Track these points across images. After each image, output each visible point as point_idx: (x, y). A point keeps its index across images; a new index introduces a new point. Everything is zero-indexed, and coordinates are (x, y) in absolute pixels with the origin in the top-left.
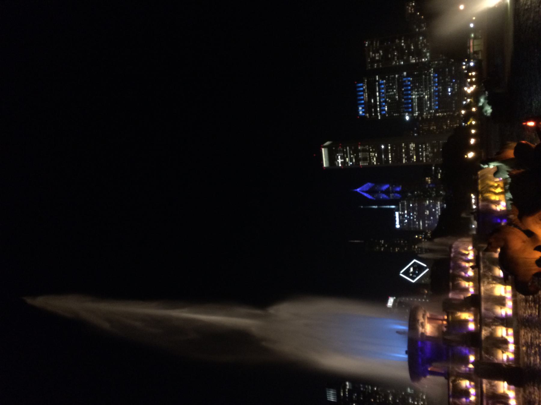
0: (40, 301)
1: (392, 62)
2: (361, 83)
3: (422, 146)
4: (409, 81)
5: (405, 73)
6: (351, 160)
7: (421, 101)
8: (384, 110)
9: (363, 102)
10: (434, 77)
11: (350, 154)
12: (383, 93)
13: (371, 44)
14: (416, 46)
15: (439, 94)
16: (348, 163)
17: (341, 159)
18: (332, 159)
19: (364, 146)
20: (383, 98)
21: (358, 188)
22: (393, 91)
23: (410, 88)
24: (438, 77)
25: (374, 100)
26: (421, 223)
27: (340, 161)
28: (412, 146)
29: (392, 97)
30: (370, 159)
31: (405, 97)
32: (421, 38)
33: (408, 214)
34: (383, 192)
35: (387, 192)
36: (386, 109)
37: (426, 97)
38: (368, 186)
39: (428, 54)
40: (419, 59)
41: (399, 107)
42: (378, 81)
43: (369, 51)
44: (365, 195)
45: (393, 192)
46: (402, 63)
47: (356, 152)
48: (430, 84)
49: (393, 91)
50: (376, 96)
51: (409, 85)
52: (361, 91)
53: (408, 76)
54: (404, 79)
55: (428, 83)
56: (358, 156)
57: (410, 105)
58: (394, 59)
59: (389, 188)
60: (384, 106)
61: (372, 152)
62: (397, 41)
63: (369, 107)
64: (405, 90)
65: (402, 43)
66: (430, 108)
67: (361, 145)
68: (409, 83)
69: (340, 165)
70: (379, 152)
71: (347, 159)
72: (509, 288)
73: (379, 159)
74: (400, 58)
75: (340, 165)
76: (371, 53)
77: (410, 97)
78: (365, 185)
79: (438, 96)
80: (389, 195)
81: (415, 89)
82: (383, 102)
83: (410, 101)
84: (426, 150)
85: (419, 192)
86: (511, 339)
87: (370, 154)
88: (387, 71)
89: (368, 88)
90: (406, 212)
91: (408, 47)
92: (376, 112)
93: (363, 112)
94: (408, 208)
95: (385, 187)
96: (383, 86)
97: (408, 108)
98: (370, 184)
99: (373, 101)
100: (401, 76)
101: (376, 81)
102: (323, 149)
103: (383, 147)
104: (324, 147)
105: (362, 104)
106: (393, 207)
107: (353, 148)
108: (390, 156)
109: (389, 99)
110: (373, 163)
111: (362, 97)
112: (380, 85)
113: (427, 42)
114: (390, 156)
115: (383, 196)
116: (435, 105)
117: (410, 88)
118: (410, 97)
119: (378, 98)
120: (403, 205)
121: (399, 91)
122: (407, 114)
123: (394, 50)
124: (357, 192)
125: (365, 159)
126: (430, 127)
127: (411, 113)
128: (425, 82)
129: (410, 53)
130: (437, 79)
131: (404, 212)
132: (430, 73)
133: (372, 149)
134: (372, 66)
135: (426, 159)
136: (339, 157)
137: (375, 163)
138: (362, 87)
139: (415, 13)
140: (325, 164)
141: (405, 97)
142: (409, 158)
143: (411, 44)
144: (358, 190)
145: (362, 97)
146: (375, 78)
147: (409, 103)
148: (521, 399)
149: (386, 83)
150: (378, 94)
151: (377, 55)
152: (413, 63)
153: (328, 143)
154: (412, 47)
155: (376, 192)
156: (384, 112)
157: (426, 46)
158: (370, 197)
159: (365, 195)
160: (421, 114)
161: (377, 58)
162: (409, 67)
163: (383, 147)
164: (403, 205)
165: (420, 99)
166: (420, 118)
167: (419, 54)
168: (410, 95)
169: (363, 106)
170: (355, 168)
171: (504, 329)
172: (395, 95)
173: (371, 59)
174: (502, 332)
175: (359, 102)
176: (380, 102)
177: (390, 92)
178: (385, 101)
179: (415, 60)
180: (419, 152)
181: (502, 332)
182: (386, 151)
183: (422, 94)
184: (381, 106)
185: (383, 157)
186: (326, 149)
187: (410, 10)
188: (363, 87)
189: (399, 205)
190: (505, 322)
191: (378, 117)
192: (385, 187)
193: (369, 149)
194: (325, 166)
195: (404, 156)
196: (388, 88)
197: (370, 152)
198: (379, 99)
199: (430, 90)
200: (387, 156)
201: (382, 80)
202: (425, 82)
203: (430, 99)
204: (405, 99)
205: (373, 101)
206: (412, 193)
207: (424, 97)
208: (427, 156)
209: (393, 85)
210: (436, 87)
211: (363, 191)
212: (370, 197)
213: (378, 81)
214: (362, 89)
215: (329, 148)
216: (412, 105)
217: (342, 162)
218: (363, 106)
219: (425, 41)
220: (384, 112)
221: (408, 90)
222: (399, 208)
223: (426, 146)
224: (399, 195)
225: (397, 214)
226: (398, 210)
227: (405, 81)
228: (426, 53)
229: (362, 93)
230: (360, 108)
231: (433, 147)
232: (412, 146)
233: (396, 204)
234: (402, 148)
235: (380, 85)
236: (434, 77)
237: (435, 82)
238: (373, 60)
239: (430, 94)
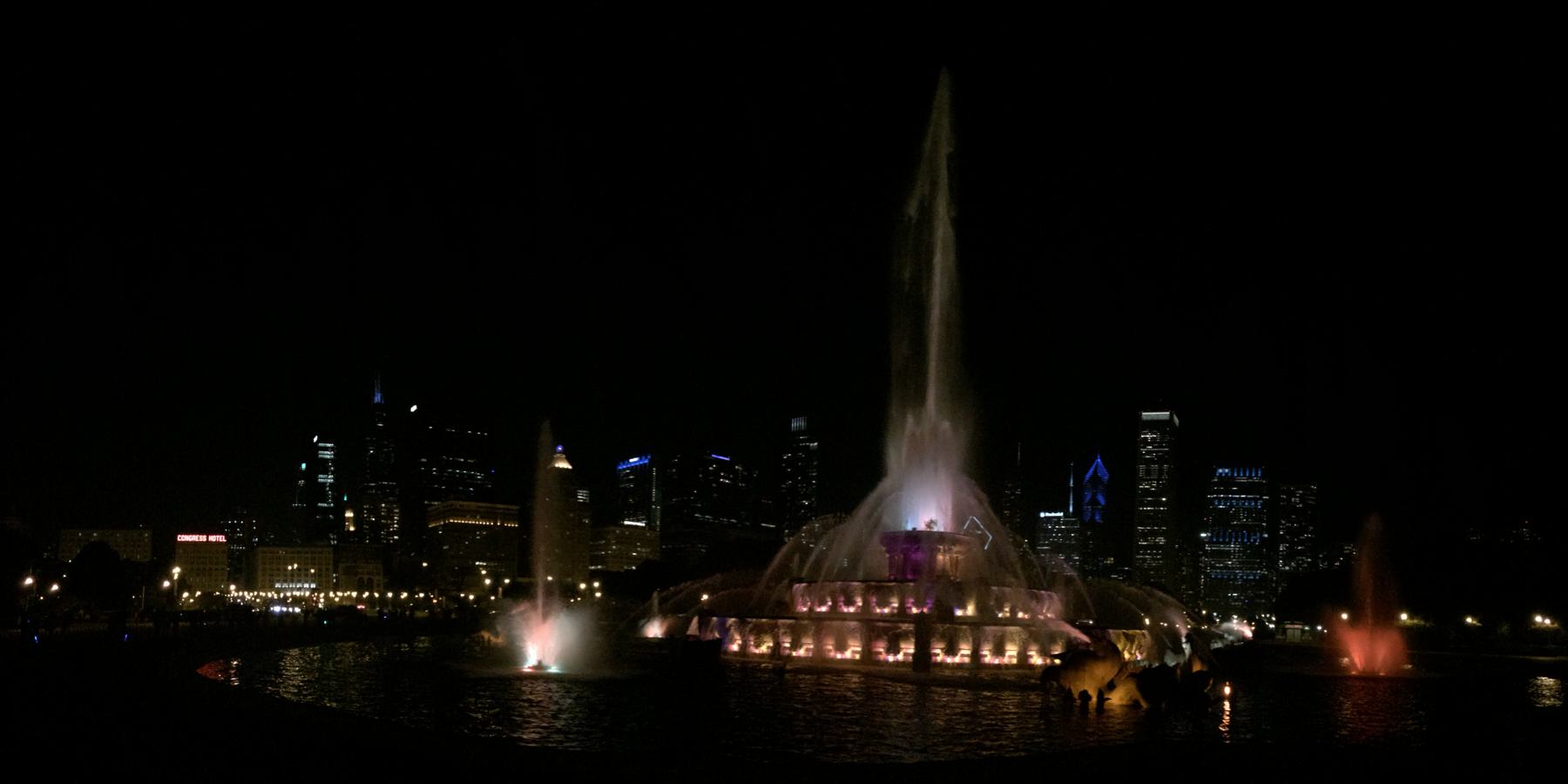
6: (1149, 452)
7: (1227, 556)
14: (1301, 553)
18: (1153, 425)
25: (1235, 489)
28: (1161, 541)
29: (1236, 516)
33: (1060, 530)
35: (1094, 502)
38: (1105, 475)
41: (1222, 524)
47: (1160, 460)
53: (1262, 539)
63: (1227, 483)
66: (1213, 567)
72: (1015, 661)
73: (1147, 492)
74: (1288, 531)
86: (957, 659)
92: (1219, 492)
94: (1069, 531)
95: (1101, 499)
100: (1263, 530)
112: (1256, 500)
120: (1073, 523)
121: (1244, 526)
125: (1148, 472)
127: (1210, 542)
129: (1293, 544)
140: (1146, 415)
142: (1144, 536)
148: (840, 667)
153: (1176, 420)
158: (1088, 476)
160: (1206, 553)
162: (1275, 540)
164: (1073, 523)
165: (1227, 554)
167: (1288, 557)
171: (1015, 653)
174: (965, 650)
181: (965, 650)
184: (1226, 499)
190: (923, 653)
192: (1101, 499)
196: (1249, 511)
203: (1226, 567)
212: (1088, 476)
215: (1170, 421)
231: (1157, 569)
232: (1161, 541)
233: (1075, 514)
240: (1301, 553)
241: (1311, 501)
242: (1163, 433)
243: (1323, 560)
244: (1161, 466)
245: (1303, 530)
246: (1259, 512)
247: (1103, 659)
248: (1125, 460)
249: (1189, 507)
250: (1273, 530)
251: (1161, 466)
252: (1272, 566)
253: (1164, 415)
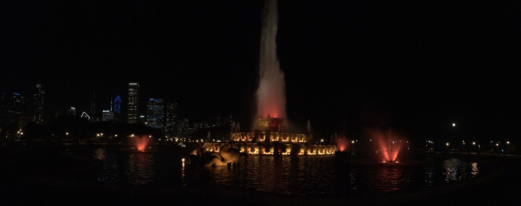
14: (173, 121)
35: (117, 108)
38: (120, 100)
47: (134, 96)
63: (152, 102)
70: (134, 106)
74: (169, 115)
95: (119, 107)
115: (116, 106)
125: (131, 100)
129: (170, 119)
142: (130, 117)
162: (166, 117)
165: (153, 121)
188: (160, 101)
192: (119, 107)
200: (132, 108)
238: (170, 106)
240: (173, 121)
248: (125, 96)
252: (165, 125)
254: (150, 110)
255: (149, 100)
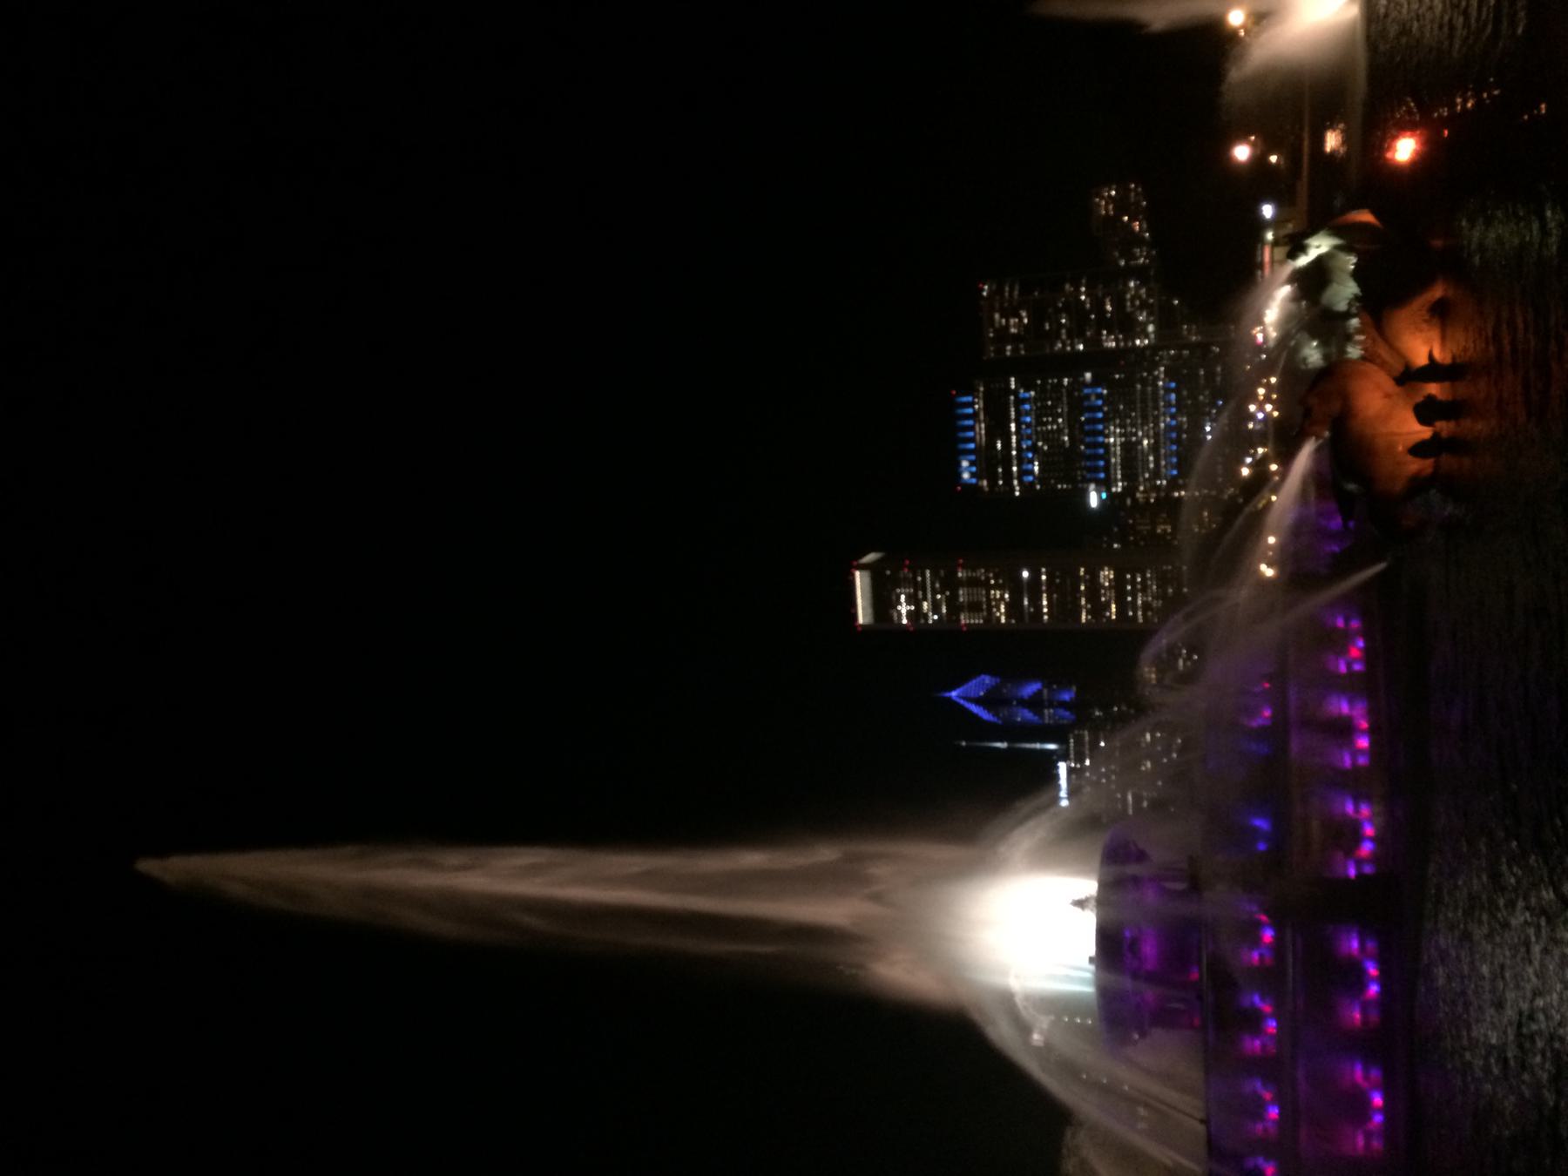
0: (173, 868)
1: (1053, 345)
2: (967, 394)
3: (1134, 578)
4: (1099, 396)
5: (1088, 376)
6: (936, 608)
8: (1031, 472)
9: (972, 446)
10: (1168, 390)
11: (934, 592)
12: (1028, 425)
13: (997, 292)
14: (1119, 303)
15: (1179, 436)
16: (926, 616)
17: (908, 602)
18: (882, 603)
19: (974, 570)
20: (1029, 437)
21: (954, 688)
22: (1055, 422)
23: (1100, 415)
24: (1177, 391)
25: (1002, 443)
26: (1130, 798)
27: (904, 609)
28: (1107, 575)
29: (1049, 437)
30: (991, 605)
31: (1088, 440)
32: (1132, 284)
34: (1024, 703)
35: (1035, 703)
36: (1036, 469)
37: (1146, 442)
38: (982, 683)
39: (1151, 328)
40: (1125, 340)
41: (1071, 465)
42: (1015, 393)
43: (992, 310)
44: (974, 709)
45: (1051, 705)
46: (1081, 347)
47: (950, 584)
48: (1156, 408)
49: (1055, 422)
50: (1009, 433)
51: (1099, 409)
52: (968, 417)
53: (1096, 382)
54: (1086, 391)
55: (1150, 404)
56: (954, 596)
57: (1102, 463)
58: (1058, 336)
59: (1040, 692)
60: (1031, 462)
61: (995, 587)
62: (1067, 287)
63: (989, 462)
64: (1088, 421)
65: (1080, 294)
66: (1156, 474)
67: (964, 567)
68: (1100, 402)
69: (905, 621)
70: (1016, 587)
71: (925, 605)
73: (1014, 608)
74: (1076, 333)
75: (905, 621)
76: (997, 316)
77: (1101, 439)
78: (973, 683)
79: (1178, 441)
80: (1041, 716)
81: (1114, 419)
82: (1029, 449)
83: (1101, 451)
84: (1144, 589)
85: (1124, 708)
87: (988, 594)
88: (1039, 365)
89: (986, 409)
90: (1087, 762)
91: (1098, 306)
92: (1008, 475)
93: (973, 475)
95: (1030, 689)
96: (1027, 407)
97: (1096, 469)
98: (987, 680)
99: (999, 445)
100: (1078, 384)
101: (1009, 391)
102: (857, 574)
103: (1025, 574)
104: (862, 567)
105: (970, 452)
106: (1052, 746)
107: (942, 573)
108: (1045, 603)
109: (1045, 441)
110: (999, 619)
111: (971, 434)
112: (1020, 402)
113: (1149, 296)
114: (1045, 603)
115: (1024, 715)
116: (1169, 465)
117: (1100, 415)
118: (1101, 439)
119: (1014, 438)
120: (1079, 741)
121: (1072, 422)
122: (1092, 486)
123: (1058, 312)
124: (950, 699)
125: (974, 607)
126: (1154, 524)
127: (1105, 484)
128: (1144, 401)
129: (1103, 322)
130: (1173, 396)
131: (1082, 762)
132: (1157, 378)
133: (996, 578)
134: (1002, 351)
135: (1144, 615)
136: (903, 597)
137: (1003, 620)
138: (971, 405)
139: (1118, 217)
140: (863, 616)
141: (1088, 440)
142: (1098, 609)
143: (1104, 297)
144: (954, 694)
145: (971, 434)
146: (1008, 384)
147: (1098, 457)
149: (1035, 399)
150: (1013, 426)
151: (1013, 321)
152: (1111, 350)
153: (870, 557)
154: (1109, 308)
155: (1005, 702)
156: (1031, 478)
157: (1144, 306)
158: (985, 715)
159: (974, 709)
160: (1130, 491)
161: (1013, 330)
162: (1099, 359)
163: (1025, 574)
164: (1079, 741)
165: (1130, 448)
166: (1129, 502)
167: (1128, 327)
168: (1101, 433)
169: (973, 457)
170: (947, 634)
172: (1060, 431)
173: (995, 331)
175: (962, 446)
176: (1019, 449)
177: (1046, 424)
178: (1034, 449)
179: (1117, 340)
180: (1126, 593)
182: (1034, 587)
183: (1135, 434)
184: (1021, 460)
185: (1026, 602)
186: (867, 574)
187: (1104, 208)
189: (1067, 743)
191: (1013, 490)
192: (1030, 689)
193: (988, 579)
194: (861, 620)
195: (1083, 601)
197: (989, 587)
198: (1018, 442)
199: (1157, 424)
200: (1036, 602)
201: (1027, 390)
202: (1144, 401)
203: (1155, 448)
204: (1088, 446)
205: (999, 445)
206: (1105, 708)
207: (1140, 442)
208: (1146, 607)
209: (1054, 407)
210: (1173, 417)
211: (965, 698)
212: (985, 715)
213: (1015, 393)
214: (970, 411)
215: (874, 570)
216: (1108, 462)
217: (909, 613)
218: (973, 457)
219: (1143, 291)
220: (1031, 478)
221: (1096, 421)
222: (1068, 749)
223: (1144, 579)
224: (1067, 715)
225: (1062, 768)
226: (1065, 758)
227: (1088, 397)
228: (1145, 324)
229: (971, 422)
230: (965, 464)
231: (1163, 581)
232: (1107, 575)
233: (1061, 738)
234: (1078, 580)
235: (1020, 402)
236: (1168, 390)
237: (1168, 405)
239: (1156, 435)
240: (1119, 303)
241: (1011, 292)
242: (897, 583)
243: (1130, 256)
244: (960, 583)
245: (1074, 309)
246: (1041, 397)
247: (1346, 398)
248: (949, 650)
249: (1044, 527)
250: (1074, 364)
251: (960, 583)
253: (860, 580)
254: (1042, 478)
255: (976, 489)
